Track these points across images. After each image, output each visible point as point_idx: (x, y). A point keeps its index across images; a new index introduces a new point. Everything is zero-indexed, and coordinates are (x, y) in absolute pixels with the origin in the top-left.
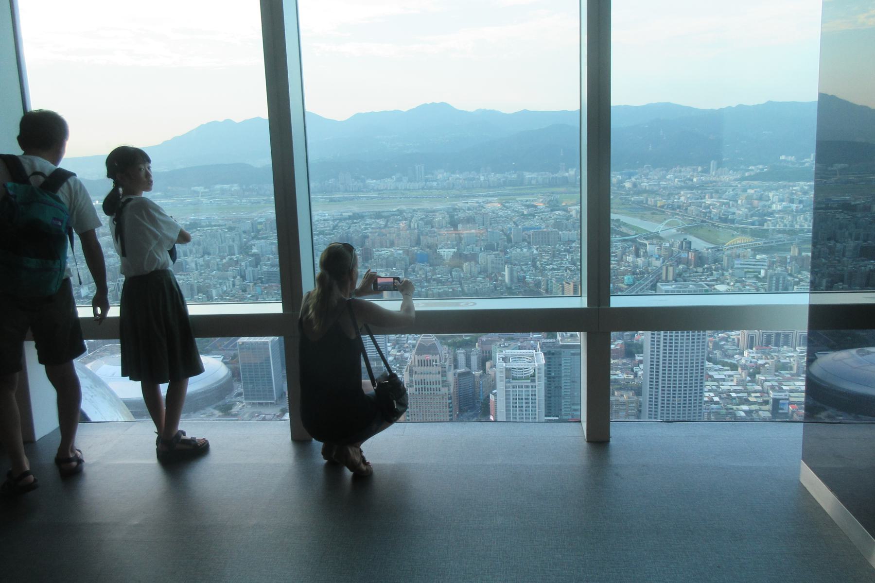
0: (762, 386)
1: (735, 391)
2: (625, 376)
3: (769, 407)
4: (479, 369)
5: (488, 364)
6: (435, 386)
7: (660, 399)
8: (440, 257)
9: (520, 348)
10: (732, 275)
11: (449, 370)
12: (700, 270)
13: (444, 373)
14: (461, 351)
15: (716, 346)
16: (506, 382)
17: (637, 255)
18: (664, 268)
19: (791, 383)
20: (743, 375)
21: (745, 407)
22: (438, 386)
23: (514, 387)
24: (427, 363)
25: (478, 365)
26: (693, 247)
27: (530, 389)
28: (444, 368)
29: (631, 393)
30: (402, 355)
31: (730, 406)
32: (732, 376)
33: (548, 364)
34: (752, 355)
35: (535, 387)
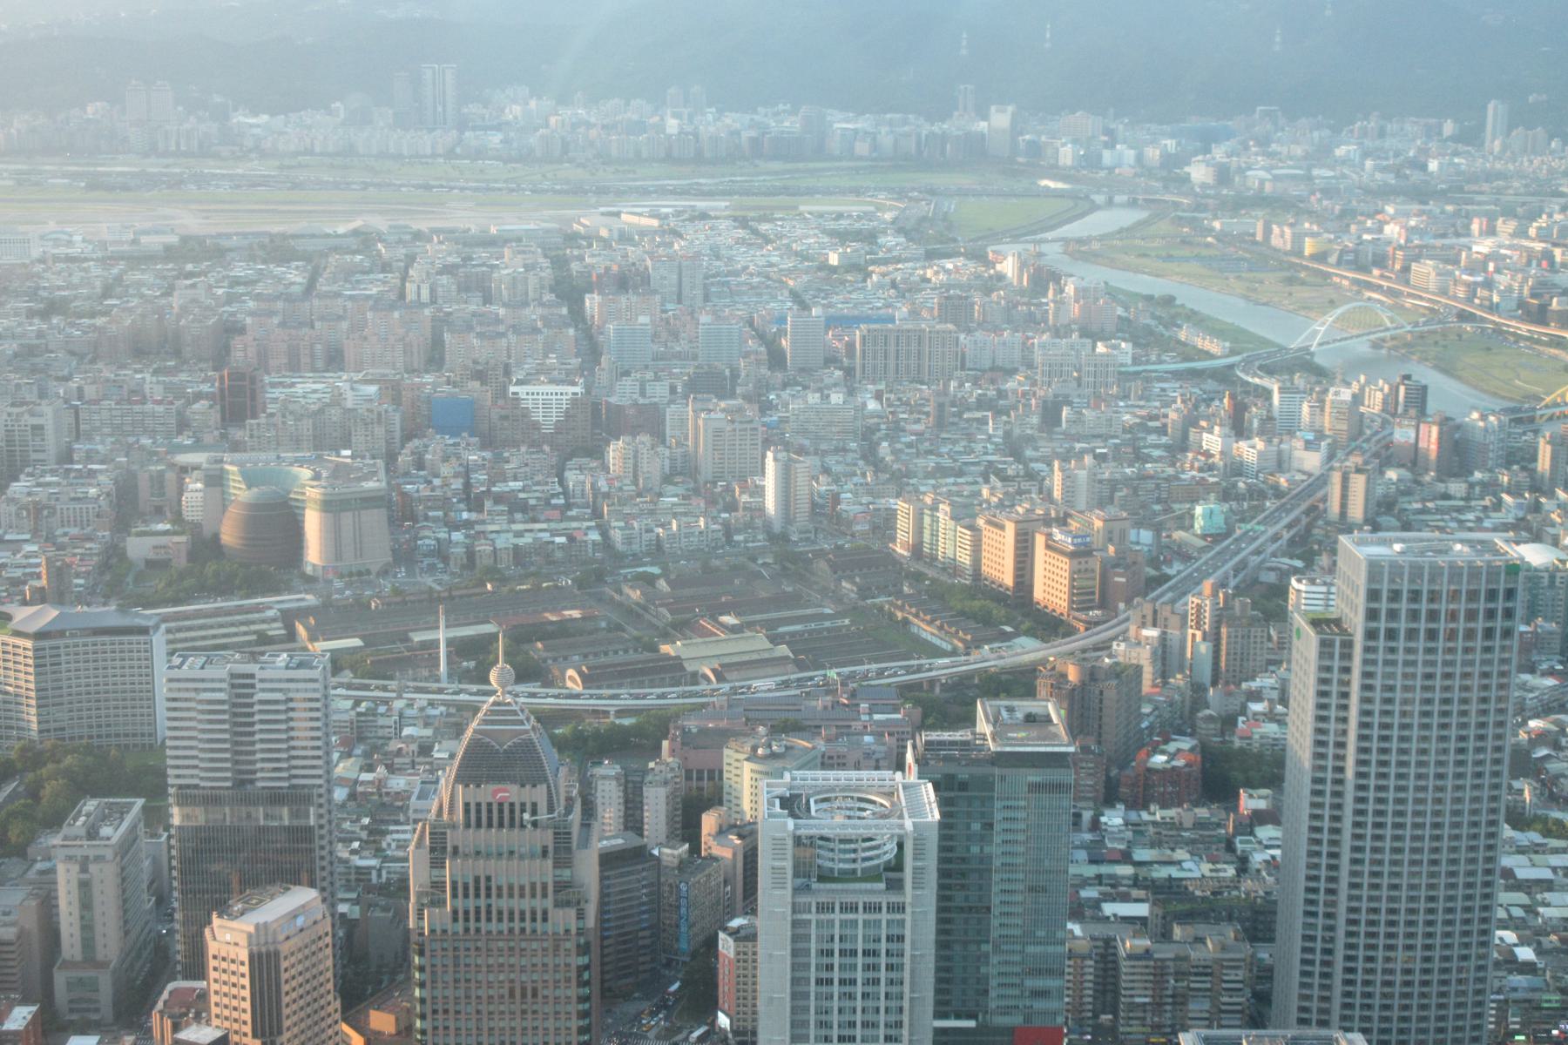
6: (526, 904)
7: (1340, 953)
8: (517, 415)
9: (827, 762)
11: (585, 843)
13: (562, 850)
14: (607, 771)
15: (1524, 764)
16: (797, 891)
17: (1239, 429)
18: (1336, 478)
22: (538, 903)
23: (823, 908)
24: (505, 817)
25: (670, 820)
27: (884, 916)
28: (562, 835)
30: (380, 784)
33: (943, 825)
35: (901, 908)
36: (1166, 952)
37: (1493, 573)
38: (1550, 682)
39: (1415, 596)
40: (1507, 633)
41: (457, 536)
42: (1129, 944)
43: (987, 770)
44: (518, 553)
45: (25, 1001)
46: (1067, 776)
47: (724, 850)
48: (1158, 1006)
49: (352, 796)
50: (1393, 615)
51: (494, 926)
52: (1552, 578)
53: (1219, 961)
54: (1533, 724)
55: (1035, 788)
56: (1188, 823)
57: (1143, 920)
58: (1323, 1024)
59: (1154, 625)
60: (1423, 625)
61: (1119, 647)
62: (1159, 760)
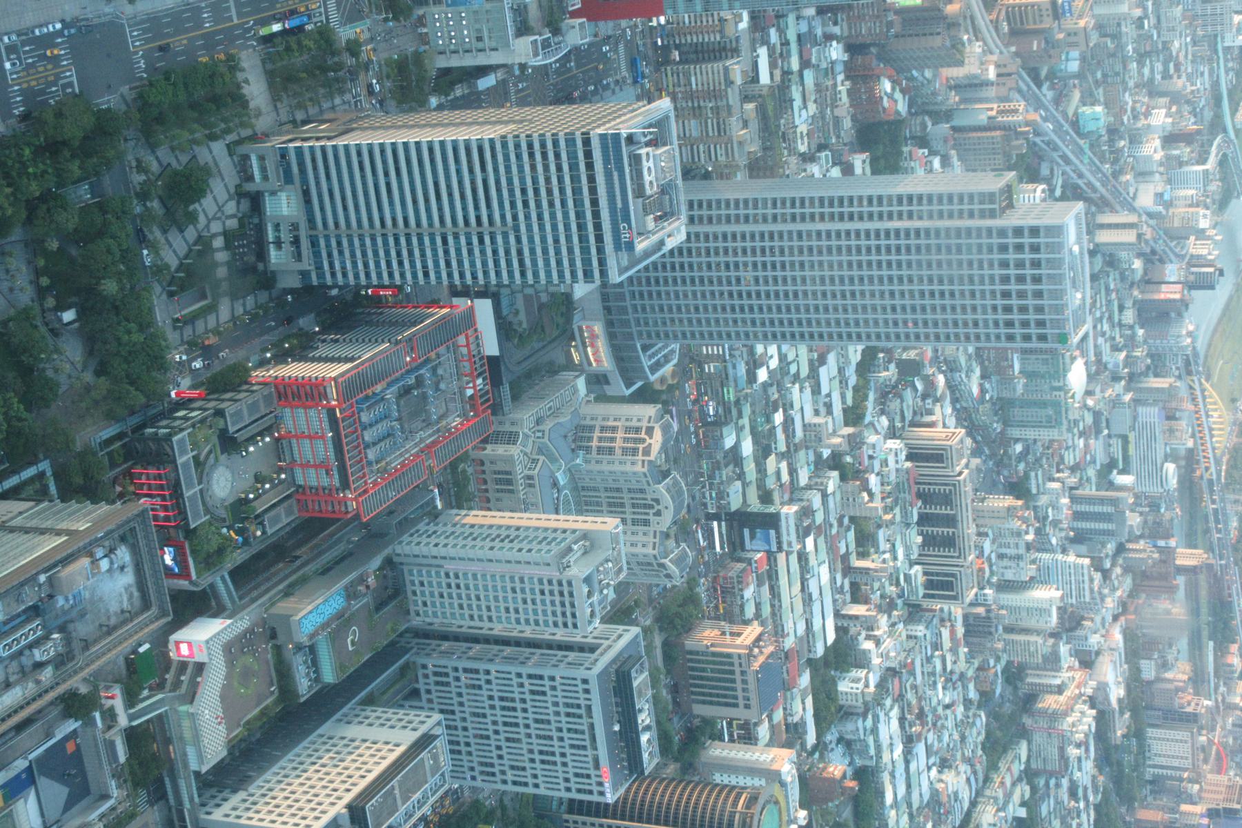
0: (809, 487)
1: (788, 422)
2: (803, 128)
3: (755, 505)
10: (1115, 403)
12: (1129, 316)
15: (909, 369)
17: (1170, 139)
18: (1133, 218)
19: (823, 555)
20: (836, 440)
21: (747, 448)
26: (1198, 294)
29: (754, 148)
31: (747, 410)
32: (829, 411)
34: (891, 460)
36: (733, 97)
37: (1059, 324)
38: (975, 391)
39: (1036, 264)
40: (1010, 338)
42: (737, 69)
48: (691, 95)
52: (1059, 389)
53: (730, 140)
54: (941, 380)
56: (837, 112)
57: (755, 79)
58: (691, 220)
59: (999, 75)
60: (1012, 272)
61: (977, 48)
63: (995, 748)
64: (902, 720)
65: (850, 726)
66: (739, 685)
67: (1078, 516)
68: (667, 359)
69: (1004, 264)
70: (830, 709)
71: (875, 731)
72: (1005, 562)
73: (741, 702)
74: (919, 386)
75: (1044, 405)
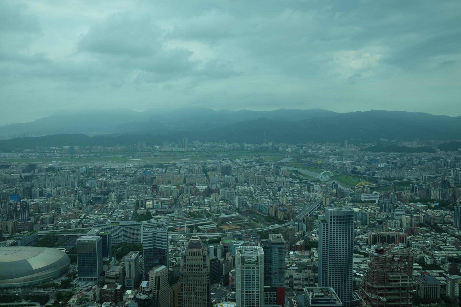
4: (221, 257)
5: (227, 254)
8: (197, 190)
13: (204, 259)
15: (356, 243)
17: (309, 191)
18: (324, 198)
23: (246, 268)
25: (221, 254)
27: (256, 269)
30: (176, 249)
33: (264, 254)
38: (359, 230)
39: (337, 217)
40: (352, 222)
41: (188, 209)
43: (271, 245)
44: (197, 212)
45: (120, 284)
46: (284, 246)
47: (230, 258)
49: (171, 251)
50: (334, 220)
51: (193, 272)
55: (278, 248)
57: (297, 270)
58: (326, 286)
62: (298, 244)
63: (440, 230)
64: (435, 250)
65: (438, 262)
66: (432, 287)
67: (385, 211)
68: (356, 295)
69: (337, 223)
70: (434, 266)
71: (439, 257)
72: (396, 226)
73: (436, 287)
74: (359, 241)
75: (362, 217)
